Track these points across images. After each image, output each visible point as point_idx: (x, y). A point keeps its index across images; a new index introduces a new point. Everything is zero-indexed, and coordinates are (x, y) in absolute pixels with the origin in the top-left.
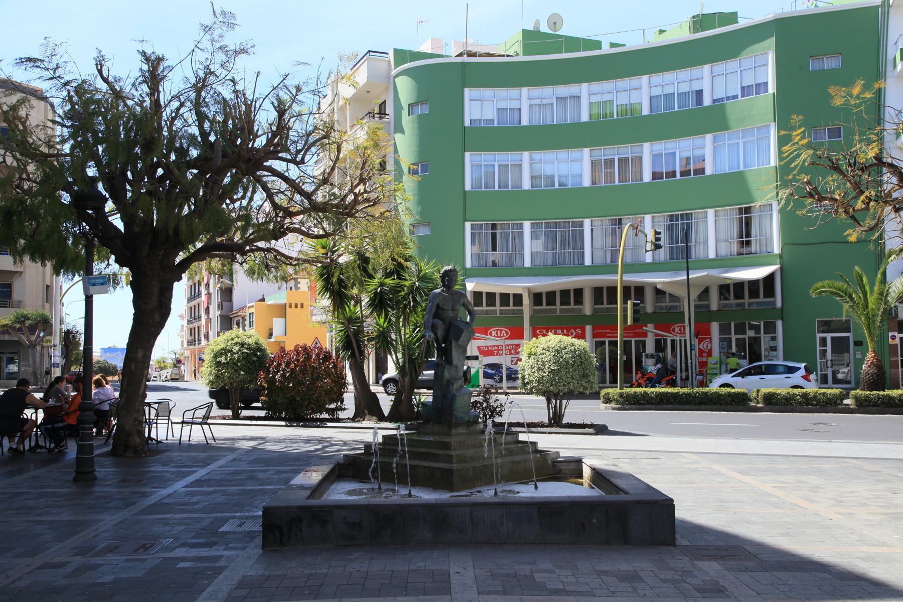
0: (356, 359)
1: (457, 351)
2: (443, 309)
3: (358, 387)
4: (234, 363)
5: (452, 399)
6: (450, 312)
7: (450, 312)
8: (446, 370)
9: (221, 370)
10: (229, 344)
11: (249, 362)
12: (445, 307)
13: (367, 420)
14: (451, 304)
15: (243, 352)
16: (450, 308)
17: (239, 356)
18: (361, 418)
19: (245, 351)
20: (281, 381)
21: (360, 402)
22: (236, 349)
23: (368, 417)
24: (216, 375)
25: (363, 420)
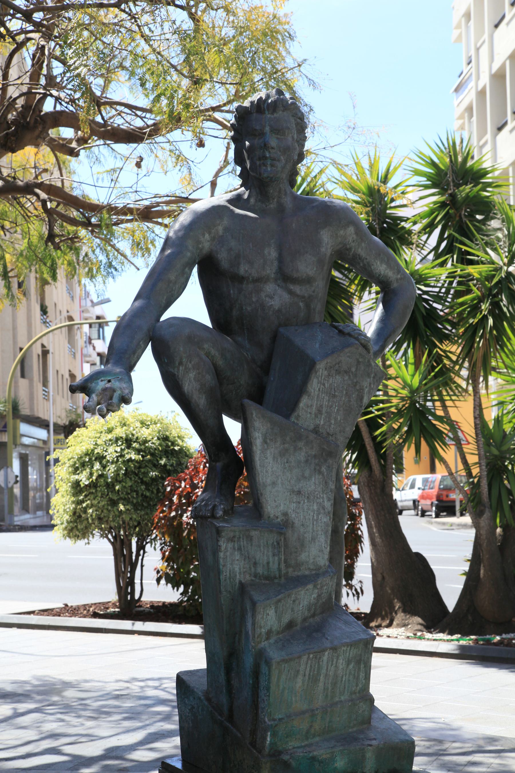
0: (370, 469)
1: (283, 453)
2: (240, 279)
3: (378, 540)
4: (107, 485)
5: (256, 673)
6: (270, 288)
7: (270, 288)
8: (223, 544)
9: (82, 502)
10: (99, 442)
11: (143, 482)
12: (243, 269)
13: (399, 626)
14: (272, 253)
15: (130, 460)
16: (271, 271)
17: (119, 469)
18: (383, 619)
19: (133, 456)
20: (192, 526)
21: (383, 578)
22: (112, 452)
23: (400, 617)
24: (74, 513)
25: (389, 625)
